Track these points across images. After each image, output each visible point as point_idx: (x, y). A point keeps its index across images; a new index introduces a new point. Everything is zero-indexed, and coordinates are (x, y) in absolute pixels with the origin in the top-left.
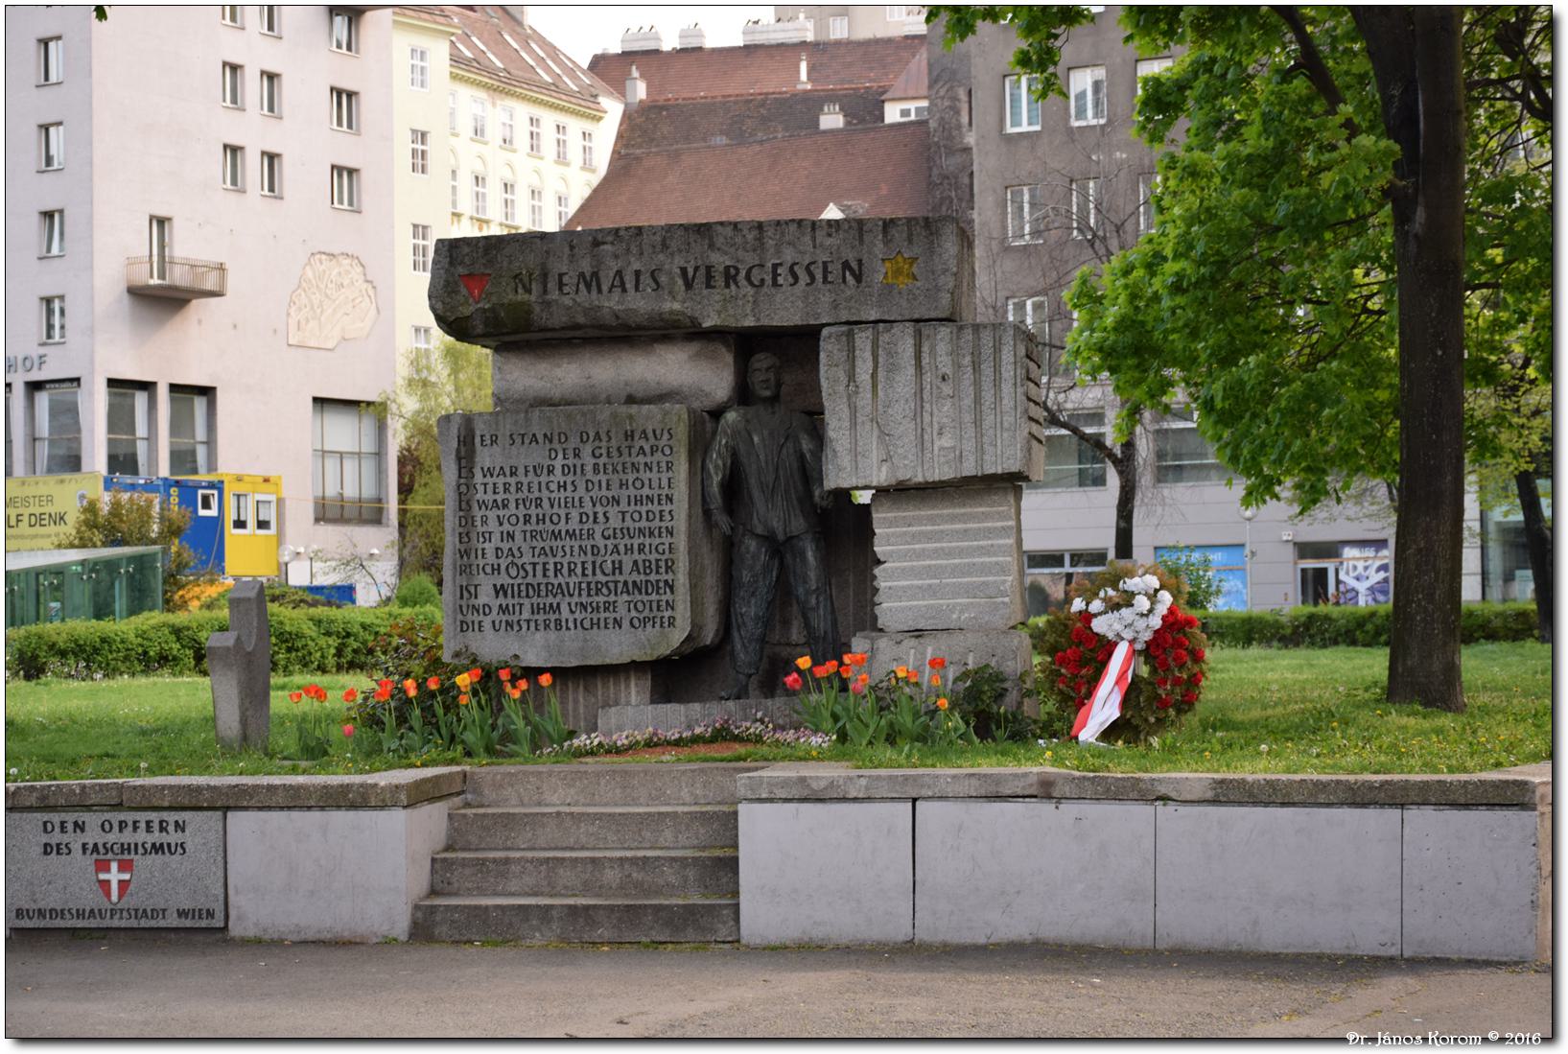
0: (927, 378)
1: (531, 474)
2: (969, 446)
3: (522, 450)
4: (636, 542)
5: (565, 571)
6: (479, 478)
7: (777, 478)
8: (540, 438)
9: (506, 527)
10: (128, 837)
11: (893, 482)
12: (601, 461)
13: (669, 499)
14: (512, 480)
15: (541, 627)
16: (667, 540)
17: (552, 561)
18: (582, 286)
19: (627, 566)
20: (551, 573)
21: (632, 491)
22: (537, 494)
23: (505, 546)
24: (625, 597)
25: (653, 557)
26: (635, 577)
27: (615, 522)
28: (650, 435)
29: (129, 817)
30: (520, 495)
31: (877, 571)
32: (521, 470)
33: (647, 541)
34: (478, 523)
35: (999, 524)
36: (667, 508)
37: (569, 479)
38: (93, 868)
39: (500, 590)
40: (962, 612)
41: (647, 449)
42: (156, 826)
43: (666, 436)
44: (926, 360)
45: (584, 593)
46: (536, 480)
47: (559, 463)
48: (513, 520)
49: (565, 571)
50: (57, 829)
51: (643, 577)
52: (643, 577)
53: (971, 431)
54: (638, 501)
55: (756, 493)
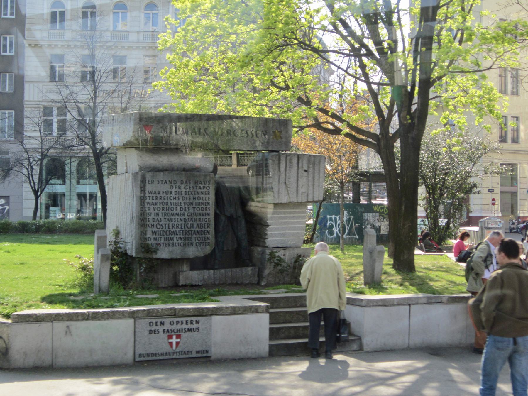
0: (300, 170)
1: (165, 194)
2: (310, 192)
3: (162, 185)
4: (198, 217)
5: (175, 227)
6: (147, 194)
8: (168, 182)
9: (156, 211)
10: (179, 326)
11: (288, 202)
13: (209, 204)
14: (158, 196)
15: (167, 245)
16: (208, 217)
19: (195, 226)
20: (171, 227)
22: (166, 201)
23: (156, 218)
24: (195, 236)
27: (191, 211)
28: (203, 183)
29: (180, 319)
30: (161, 201)
31: (268, 229)
32: (161, 193)
33: (202, 217)
34: (147, 210)
35: (303, 215)
36: (208, 207)
37: (177, 196)
38: (166, 338)
39: (154, 233)
40: (291, 242)
42: (189, 322)
43: (208, 183)
44: (300, 165)
47: (174, 190)
48: (159, 209)
49: (175, 227)
50: (154, 325)
51: (200, 229)
52: (200, 229)
53: (311, 188)
54: (199, 204)
55: (226, 202)
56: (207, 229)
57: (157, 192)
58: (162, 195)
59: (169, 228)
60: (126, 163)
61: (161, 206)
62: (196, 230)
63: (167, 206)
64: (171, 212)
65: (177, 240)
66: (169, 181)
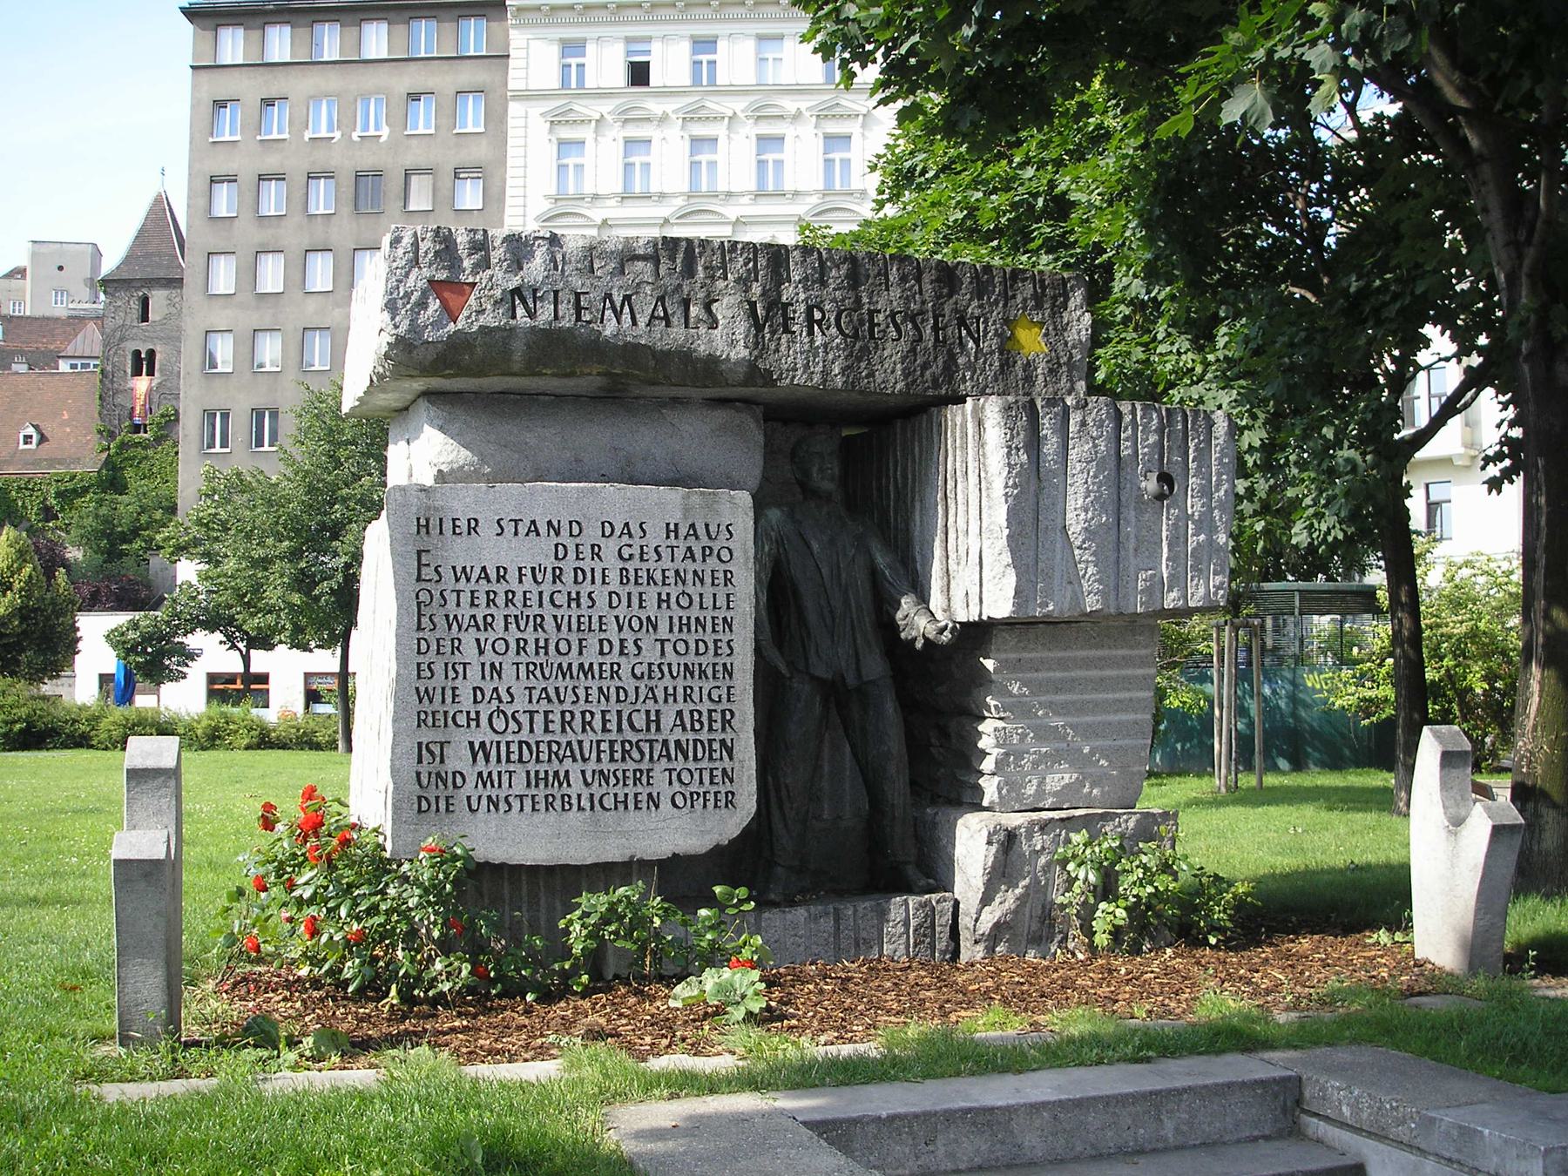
4: (680, 683)
7: (846, 602)
8: (543, 529)
12: (631, 566)
14: (501, 588)
17: (557, 708)
18: (608, 313)
21: (677, 612)
23: (488, 688)
26: (678, 734)
27: (651, 654)
28: (701, 531)
30: (512, 611)
32: (513, 575)
33: (696, 684)
37: (586, 588)
39: (479, 751)
41: (698, 556)
45: (605, 757)
46: (535, 589)
48: (500, 646)
51: (691, 736)
52: (691, 736)
54: (684, 625)
55: (812, 617)
57: (493, 576)
58: (514, 585)
59: (546, 730)
60: (411, 469)
61: (514, 633)
64: (560, 659)
65: (587, 784)
66: (550, 523)
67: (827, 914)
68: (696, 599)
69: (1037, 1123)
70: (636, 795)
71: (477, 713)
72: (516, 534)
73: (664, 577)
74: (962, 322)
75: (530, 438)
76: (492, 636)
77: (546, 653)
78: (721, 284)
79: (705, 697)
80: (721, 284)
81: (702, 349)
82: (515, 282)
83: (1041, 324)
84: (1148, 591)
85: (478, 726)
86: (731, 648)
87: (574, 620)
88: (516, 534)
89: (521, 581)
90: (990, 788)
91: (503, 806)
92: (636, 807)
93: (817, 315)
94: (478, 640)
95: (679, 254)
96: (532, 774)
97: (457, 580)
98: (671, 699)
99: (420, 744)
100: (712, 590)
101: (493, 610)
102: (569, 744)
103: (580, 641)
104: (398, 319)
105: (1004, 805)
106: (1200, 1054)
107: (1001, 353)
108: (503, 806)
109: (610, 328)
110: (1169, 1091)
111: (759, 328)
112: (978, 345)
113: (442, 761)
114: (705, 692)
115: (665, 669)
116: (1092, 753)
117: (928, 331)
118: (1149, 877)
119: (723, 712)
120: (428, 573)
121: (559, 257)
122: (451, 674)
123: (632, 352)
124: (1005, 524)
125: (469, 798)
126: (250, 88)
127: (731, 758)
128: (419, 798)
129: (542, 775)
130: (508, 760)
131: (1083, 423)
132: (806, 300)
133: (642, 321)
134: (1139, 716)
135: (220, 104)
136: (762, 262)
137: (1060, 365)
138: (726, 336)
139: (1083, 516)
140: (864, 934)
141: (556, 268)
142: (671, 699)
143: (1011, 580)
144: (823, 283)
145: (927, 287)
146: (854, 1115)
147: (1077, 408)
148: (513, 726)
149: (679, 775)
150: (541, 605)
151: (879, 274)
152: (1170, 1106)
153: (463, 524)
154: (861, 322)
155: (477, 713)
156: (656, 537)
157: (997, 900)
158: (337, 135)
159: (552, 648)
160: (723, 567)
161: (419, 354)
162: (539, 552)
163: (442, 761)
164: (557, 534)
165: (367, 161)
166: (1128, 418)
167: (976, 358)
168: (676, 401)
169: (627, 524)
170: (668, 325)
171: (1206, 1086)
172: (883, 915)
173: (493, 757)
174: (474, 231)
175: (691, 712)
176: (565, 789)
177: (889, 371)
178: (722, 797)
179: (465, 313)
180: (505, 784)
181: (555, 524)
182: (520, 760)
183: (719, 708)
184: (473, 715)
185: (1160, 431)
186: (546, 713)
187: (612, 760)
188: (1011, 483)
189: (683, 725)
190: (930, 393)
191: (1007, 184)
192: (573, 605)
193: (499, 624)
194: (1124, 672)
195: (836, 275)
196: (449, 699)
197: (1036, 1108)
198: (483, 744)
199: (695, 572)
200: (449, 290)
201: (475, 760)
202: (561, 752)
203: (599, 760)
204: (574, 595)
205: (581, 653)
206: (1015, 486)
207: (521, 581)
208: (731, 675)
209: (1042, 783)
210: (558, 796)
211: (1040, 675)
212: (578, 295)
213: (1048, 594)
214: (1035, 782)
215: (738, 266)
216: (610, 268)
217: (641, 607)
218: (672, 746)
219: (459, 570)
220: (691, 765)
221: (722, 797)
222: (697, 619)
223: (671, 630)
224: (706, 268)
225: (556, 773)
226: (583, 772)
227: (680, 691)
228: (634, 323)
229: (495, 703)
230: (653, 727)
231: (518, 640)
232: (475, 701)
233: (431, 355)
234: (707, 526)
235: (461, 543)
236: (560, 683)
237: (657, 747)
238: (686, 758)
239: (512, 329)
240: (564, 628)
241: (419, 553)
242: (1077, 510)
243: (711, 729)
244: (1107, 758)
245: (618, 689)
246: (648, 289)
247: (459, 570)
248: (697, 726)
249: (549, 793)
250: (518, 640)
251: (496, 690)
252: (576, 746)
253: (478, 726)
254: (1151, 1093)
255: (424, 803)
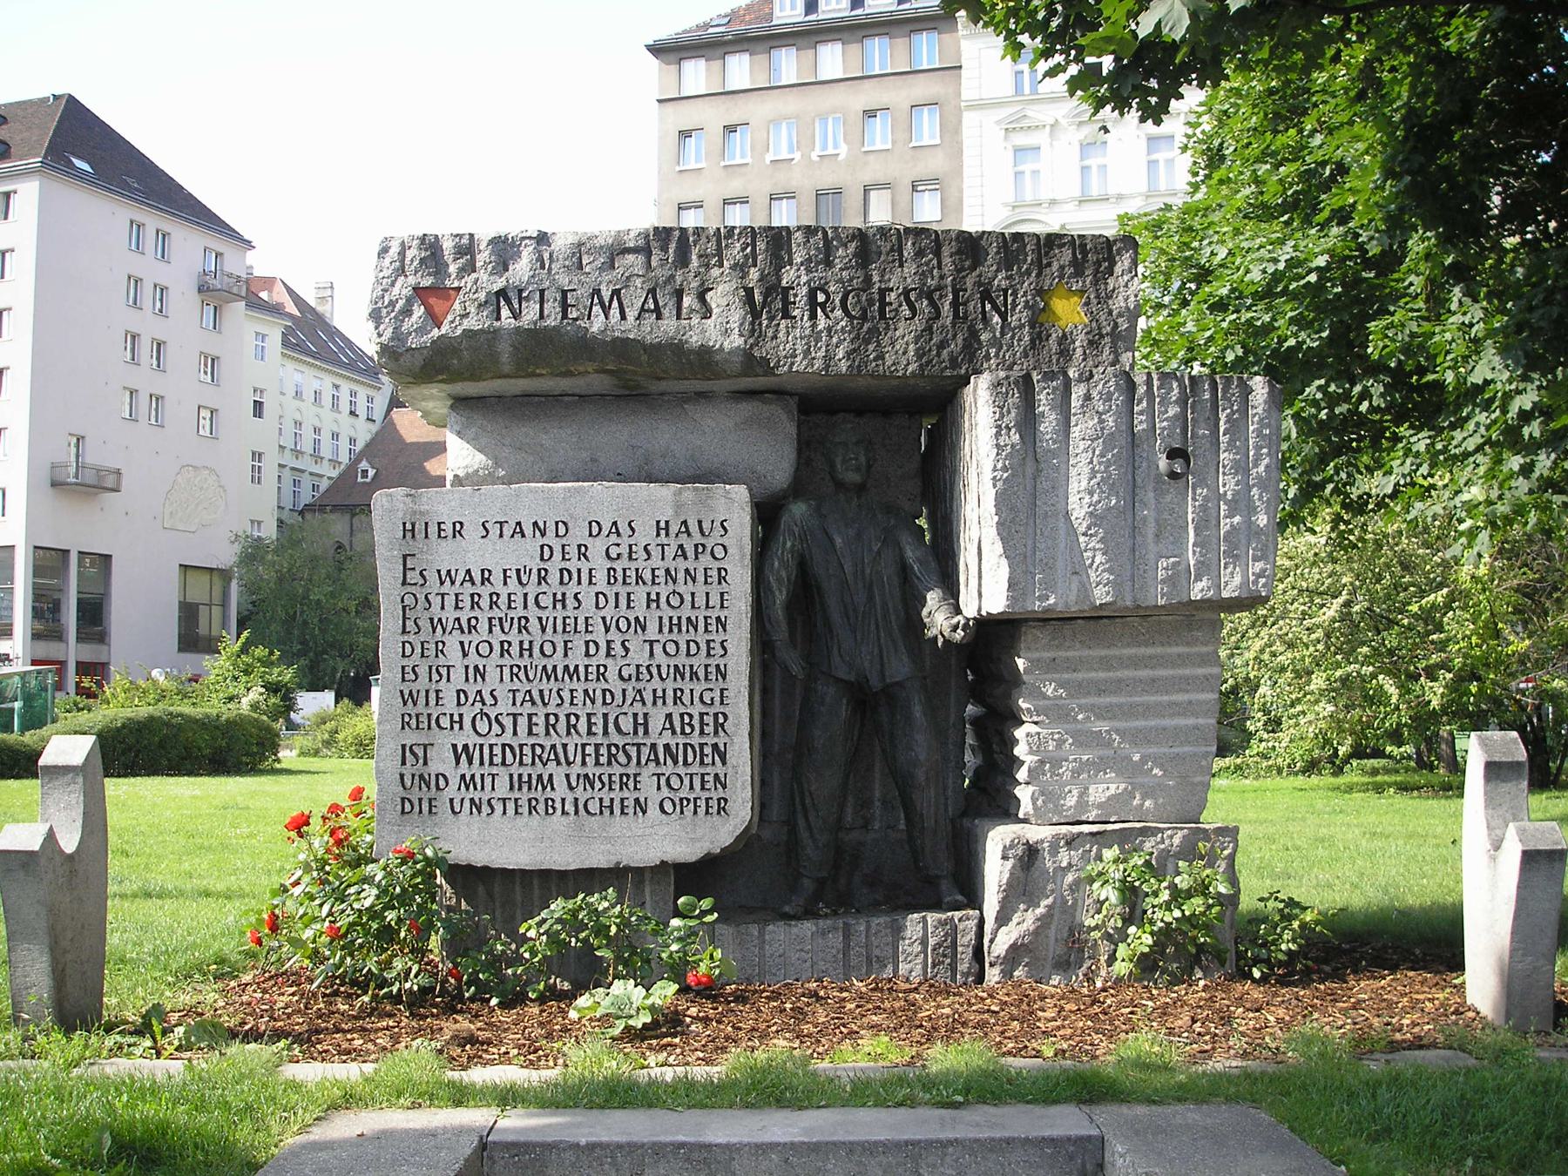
3: (500, 543)
4: (670, 686)
8: (528, 530)
9: (473, 659)
12: (619, 566)
14: (485, 591)
17: (541, 711)
18: (597, 309)
19: (657, 722)
21: (666, 612)
23: (472, 690)
25: (696, 710)
26: (667, 738)
27: (639, 655)
28: (694, 528)
30: (496, 613)
32: (497, 578)
33: (687, 686)
39: (462, 754)
41: (690, 553)
45: (590, 761)
46: (520, 591)
47: (556, 564)
48: (484, 649)
51: (681, 740)
52: (681, 740)
54: (676, 626)
55: (836, 616)
56: (711, 740)
58: (499, 587)
59: (530, 733)
62: (660, 743)
63: (526, 637)
64: (544, 661)
65: (571, 788)
66: (535, 524)
67: (836, 929)
68: (688, 598)
69: (764, 1165)
70: (622, 800)
71: (461, 715)
72: (501, 536)
73: (654, 576)
74: (986, 296)
75: (545, 439)
76: (476, 638)
77: (531, 655)
78: (715, 272)
79: (696, 700)
80: (715, 272)
81: (694, 340)
82: (500, 283)
83: (1082, 292)
84: (1171, 581)
85: (461, 728)
86: (724, 648)
87: (560, 622)
88: (501, 536)
89: (505, 583)
90: (1024, 794)
91: (485, 809)
92: (622, 813)
93: (821, 298)
94: (462, 643)
95: (671, 244)
96: (516, 778)
97: (442, 583)
98: (660, 702)
99: (404, 746)
100: (705, 589)
101: (477, 613)
102: (553, 747)
103: (566, 642)
104: (382, 327)
105: (1040, 817)
106: (1028, 1102)
107: (1032, 327)
108: (485, 809)
109: (597, 324)
110: (930, 1144)
111: (756, 314)
112: (1004, 319)
113: (425, 763)
114: (696, 695)
115: (654, 671)
116: (1144, 760)
117: (946, 307)
118: (1178, 896)
119: (716, 715)
120: (413, 577)
121: (546, 256)
122: (435, 677)
123: (622, 348)
124: (993, 510)
125: (451, 800)
126: (712, 116)
127: (724, 763)
128: (403, 799)
129: (525, 778)
130: (491, 763)
131: (1088, 397)
132: (808, 282)
133: (631, 314)
134: (1201, 721)
135: (685, 134)
136: (761, 245)
137: (1102, 336)
138: (720, 326)
139: (1087, 499)
140: (877, 952)
141: (543, 267)
142: (660, 702)
143: (1004, 571)
144: (829, 264)
145: (947, 260)
146: (550, 1139)
147: (1080, 381)
148: (496, 728)
149: (668, 780)
150: (525, 607)
151: (892, 250)
152: (931, 1159)
153: (448, 527)
154: (871, 302)
155: (461, 715)
156: (645, 535)
157: (1015, 919)
158: (797, 156)
159: (536, 651)
160: (717, 564)
161: (406, 360)
162: (525, 553)
163: (425, 763)
164: (543, 535)
165: (827, 180)
166: (1142, 390)
167: (1003, 334)
168: (702, 396)
169: (615, 523)
170: (659, 317)
171: (977, 1140)
172: (897, 931)
173: (476, 760)
174: (460, 236)
175: (682, 715)
176: (549, 793)
177: (901, 352)
178: (714, 803)
179: (450, 317)
180: (488, 787)
181: (541, 525)
182: (503, 763)
183: (712, 711)
184: (456, 718)
185: (1182, 402)
186: (530, 716)
187: (597, 763)
188: (1000, 465)
189: (672, 728)
190: (948, 373)
191: (1297, 152)
192: (559, 606)
193: (483, 626)
194: (1180, 672)
195: (842, 255)
196: (432, 702)
197: (762, 1149)
198: (466, 747)
199: (687, 571)
200: (433, 296)
201: (458, 762)
202: (545, 756)
203: (584, 763)
204: (559, 597)
205: (566, 655)
206: (1005, 469)
207: (505, 583)
208: (724, 678)
209: (1084, 793)
210: (542, 800)
211: (1080, 676)
212: (564, 293)
213: (1050, 586)
214: (1075, 792)
215: (735, 252)
216: (598, 263)
217: (629, 607)
218: (661, 750)
219: (443, 573)
220: (681, 770)
221: (714, 803)
222: (689, 619)
223: (660, 631)
224: (700, 256)
225: (540, 777)
226: (567, 776)
227: (670, 693)
228: (623, 317)
229: (478, 705)
230: (641, 730)
231: (502, 643)
232: (459, 704)
233: (419, 361)
234: (700, 522)
235: (448, 546)
236: (545, 685)
237: (645, 751)
238: (676, 762)
239: (496, 331)
240: (549, 630)
241: (405, 557)
242: (1080, 493)
243: (702, 732)
244: (1161, 767)
245: (604, 691)
246: (638, 282)
247: (443, 573)
248: (688, 730)
249: (532, 796)
250: (502, 643)
251: (479, 692)
252: (560, 750)
253: (461, 728)
254: (907, 1143)
255: (407, 805)
